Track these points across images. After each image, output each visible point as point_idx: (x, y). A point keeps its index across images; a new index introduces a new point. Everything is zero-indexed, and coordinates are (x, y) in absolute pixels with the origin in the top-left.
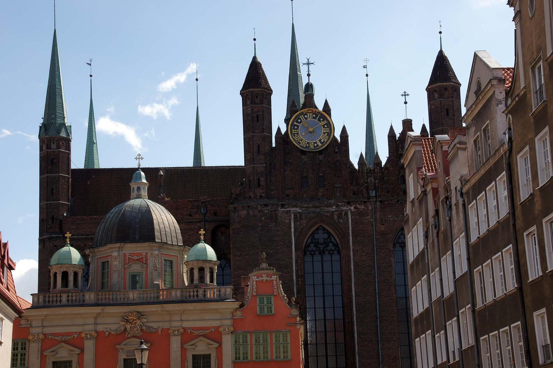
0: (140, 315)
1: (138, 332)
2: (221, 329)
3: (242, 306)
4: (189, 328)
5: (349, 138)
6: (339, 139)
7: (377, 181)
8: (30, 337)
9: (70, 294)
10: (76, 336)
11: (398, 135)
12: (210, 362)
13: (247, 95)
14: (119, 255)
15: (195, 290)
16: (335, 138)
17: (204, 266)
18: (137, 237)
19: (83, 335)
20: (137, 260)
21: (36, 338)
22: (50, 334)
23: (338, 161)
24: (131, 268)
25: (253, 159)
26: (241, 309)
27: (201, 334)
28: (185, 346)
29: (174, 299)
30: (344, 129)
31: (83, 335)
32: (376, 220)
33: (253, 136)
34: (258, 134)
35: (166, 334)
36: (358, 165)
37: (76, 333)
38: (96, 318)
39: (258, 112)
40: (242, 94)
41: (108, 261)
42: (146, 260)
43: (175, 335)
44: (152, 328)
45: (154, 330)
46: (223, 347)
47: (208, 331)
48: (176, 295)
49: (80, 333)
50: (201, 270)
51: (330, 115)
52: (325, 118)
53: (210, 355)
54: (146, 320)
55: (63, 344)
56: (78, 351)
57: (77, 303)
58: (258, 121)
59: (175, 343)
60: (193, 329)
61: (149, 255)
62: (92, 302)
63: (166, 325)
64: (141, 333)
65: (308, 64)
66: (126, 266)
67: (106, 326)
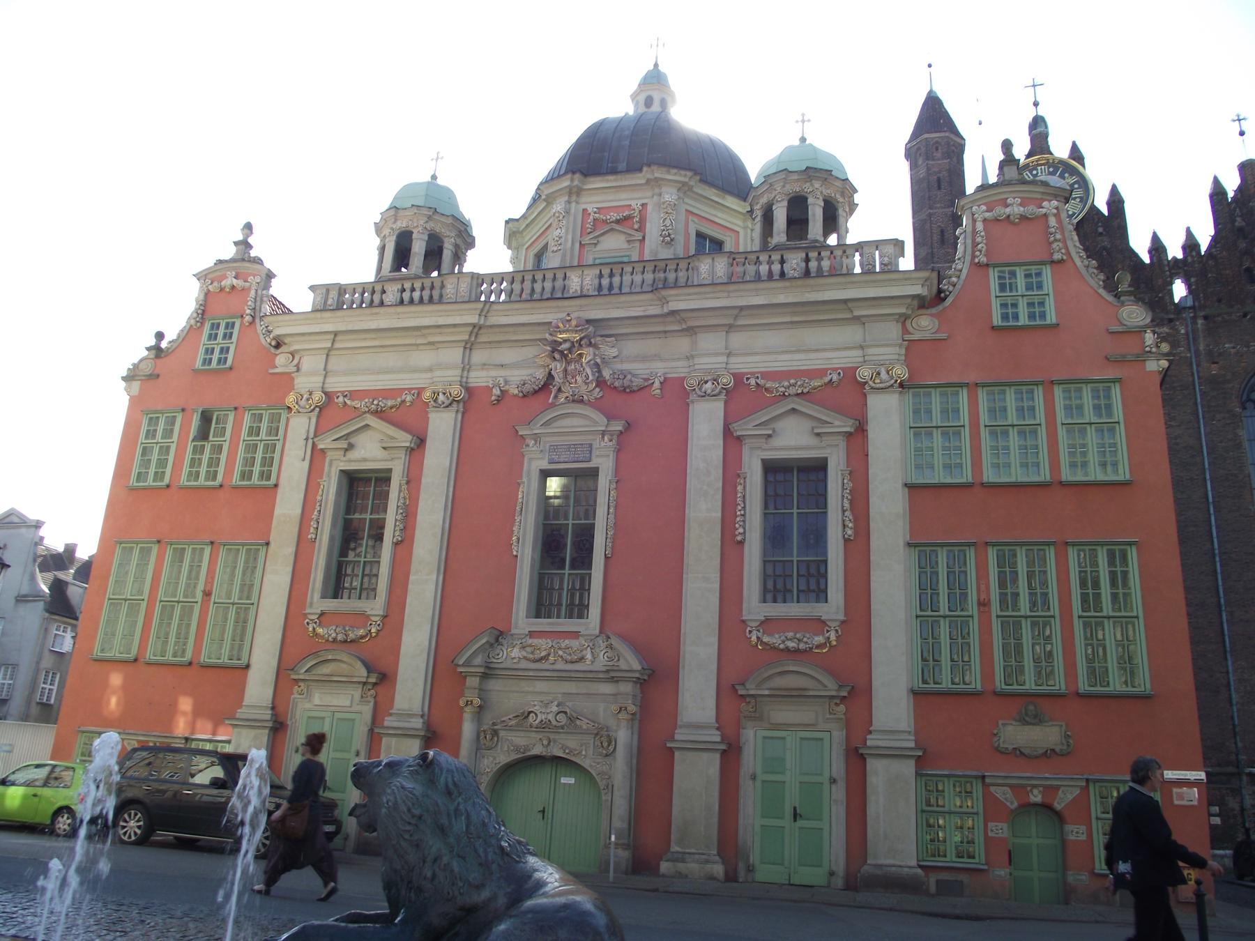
0: (595, 331)
1: (582, 384)
2: (864, 373)
3: (940, 297)
5: (1126, 206)
6: (1105, 210)
7: (1193, 280)
8: (290, 399)
9: (407, 285)
10: (409, 398)
11: (1231, 194)
12: (824, 496)
13: (919, 149)
14: (567, 212)
15: (776, 257)
16: (1094, 208)
17: (807, 187)
18: (622, 166)
20: (618, 222)
21: (303, 403)
22: (342, 392)
23: (1104, 248)
24: (599, 248)
25: (932, 253)
27: (792, 391)
28: (739, 429)
30: (1114, 192)
31: (427, 395)
32: (1197, 352)
33: (930, 215)
34: (941, 211)
35: (678, 394)
36: (1150, 252)
37: (410, 389)
38: (469, 346)
39: (940, 172)
40: (909, 154)
41: (546, 247)
42: (642, 222)
43: (705, 395)
44: (634, 375)
45: (637, 382)
46: (871, 435)
47: (817, 383)
48: (712, 272)
49: (420, 391)
50: (798, 205)
51: (1083, 165)
52: (1074, 172)
53: (826, 459)
54: (614, 352)
55: (371, 420)
56: (405, 439)
58: (939, 188)
59: (705, 422)
60: (766, 375)
61: (649, 208)
63: (678, 369)
64: (597, 393)
65: (1034, 86)
66: (586, 240)
67: (494, 373)
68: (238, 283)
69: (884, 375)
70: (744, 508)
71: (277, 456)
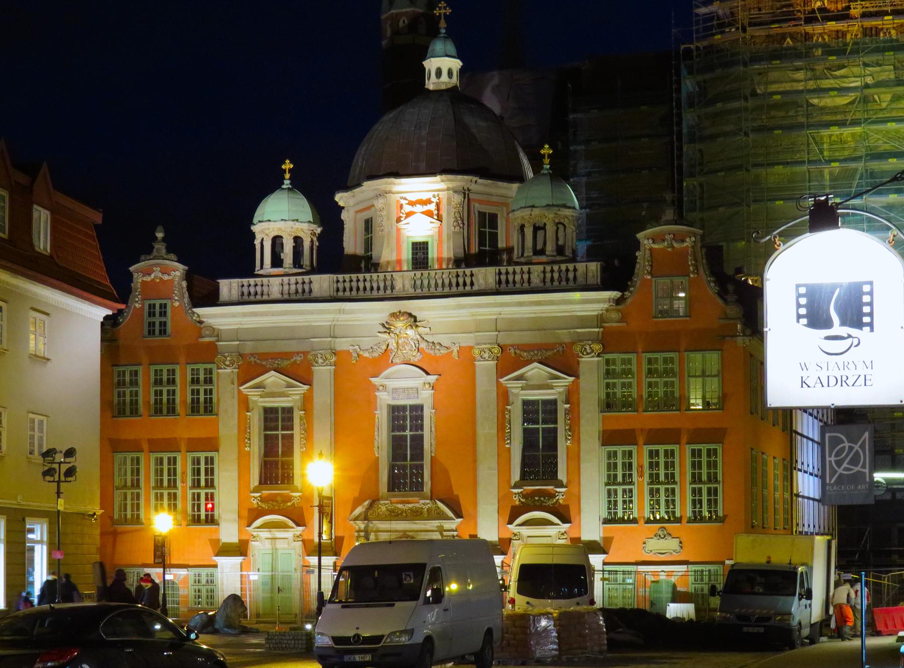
4: (512, 346)
15: (525, 268)
19: (310, 357)
26: (620, 307)
29: (483, 287)
47: (549, 353)
48: (485, 279)
57: (299, 296)
62: (326, 294)
68: (166, 277)
69: (588, 347)
70: (510, 428)
71: (215, 397)
